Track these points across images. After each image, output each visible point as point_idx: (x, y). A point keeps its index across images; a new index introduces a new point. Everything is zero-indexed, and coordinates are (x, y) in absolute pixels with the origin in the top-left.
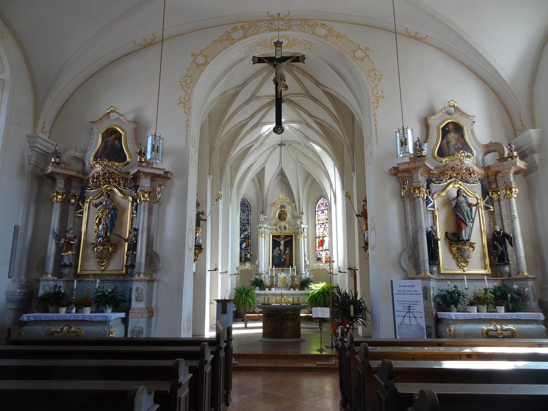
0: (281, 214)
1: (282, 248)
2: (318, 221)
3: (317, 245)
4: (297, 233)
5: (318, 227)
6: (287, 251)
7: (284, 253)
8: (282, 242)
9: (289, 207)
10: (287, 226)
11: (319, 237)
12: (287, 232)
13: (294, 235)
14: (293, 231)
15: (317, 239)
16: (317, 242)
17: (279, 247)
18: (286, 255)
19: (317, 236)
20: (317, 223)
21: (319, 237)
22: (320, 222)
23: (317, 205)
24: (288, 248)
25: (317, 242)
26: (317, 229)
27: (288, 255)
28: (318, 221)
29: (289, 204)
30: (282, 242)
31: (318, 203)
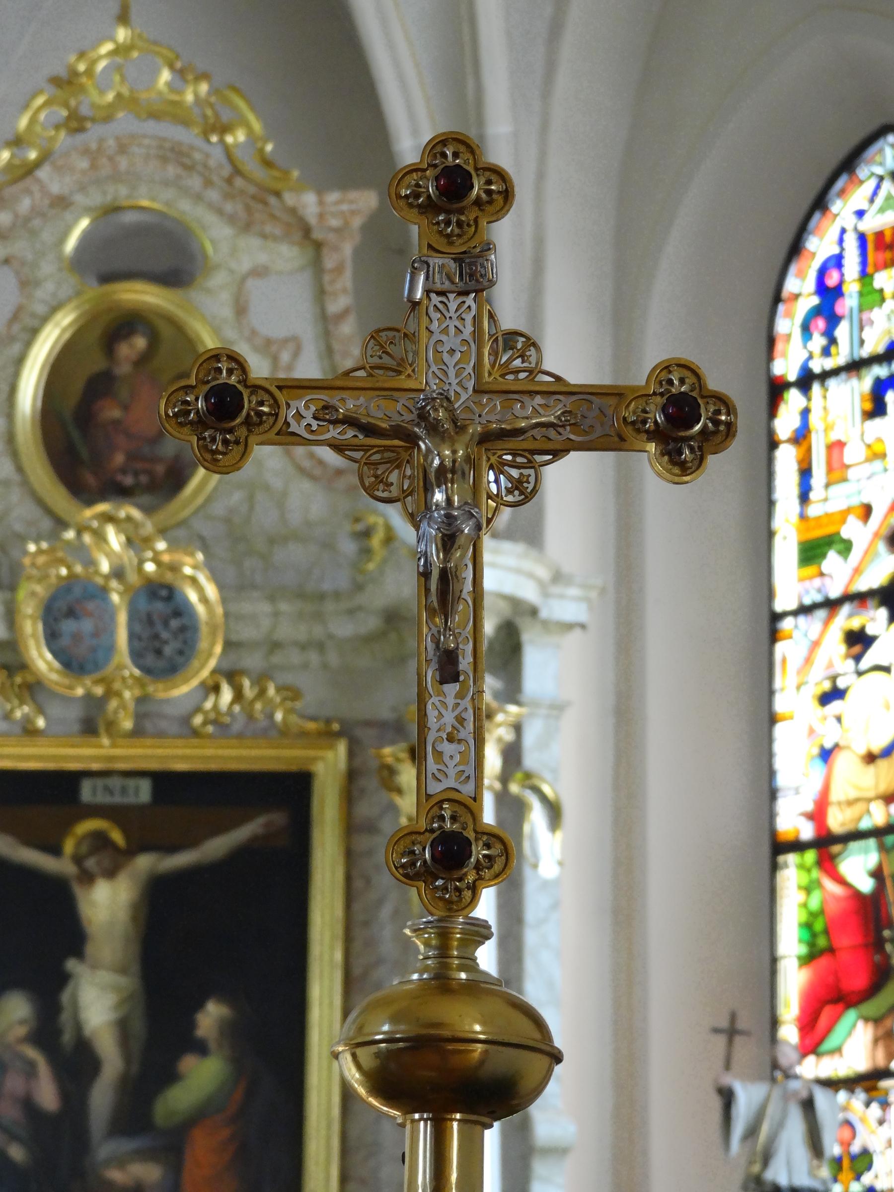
0: (101, 385)
1: (97, 1002)
2: (812, 552)
3: (793, 983)
4: (393, 729)
5: (806, 653)
6: (202, 1077)
7: (135, 1112)
8: (107, 903)
9: (252, 252)
10: (202, 594)
11: (827, 845)
12: (206, 718)
13: (329, 765)
14: (316, 694)
15: (794, 873)
16: (790, 943)
17: (48, 988)
18: (171, 1146)
19: (792, 821)
20: (790, 585)
21: (827, 845)
22: (836, 574)
23: (801, 284)
24: (211, 1016)
25: (790, 943)
26: (793, 696)
27: (205, 1151)
28: (812, 552)
29: (256, 199)
30: (107, 903)
31: (820, 245)
